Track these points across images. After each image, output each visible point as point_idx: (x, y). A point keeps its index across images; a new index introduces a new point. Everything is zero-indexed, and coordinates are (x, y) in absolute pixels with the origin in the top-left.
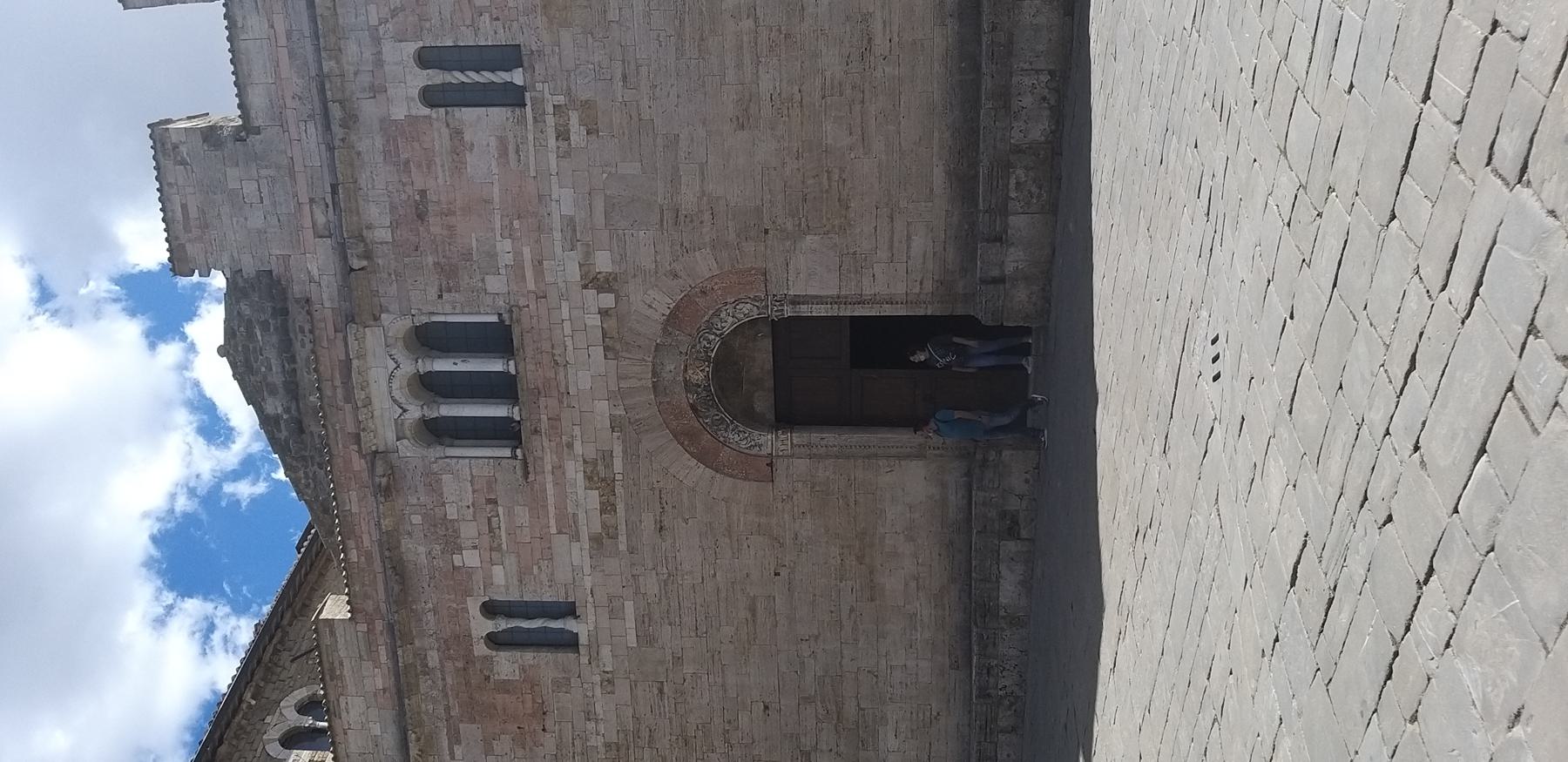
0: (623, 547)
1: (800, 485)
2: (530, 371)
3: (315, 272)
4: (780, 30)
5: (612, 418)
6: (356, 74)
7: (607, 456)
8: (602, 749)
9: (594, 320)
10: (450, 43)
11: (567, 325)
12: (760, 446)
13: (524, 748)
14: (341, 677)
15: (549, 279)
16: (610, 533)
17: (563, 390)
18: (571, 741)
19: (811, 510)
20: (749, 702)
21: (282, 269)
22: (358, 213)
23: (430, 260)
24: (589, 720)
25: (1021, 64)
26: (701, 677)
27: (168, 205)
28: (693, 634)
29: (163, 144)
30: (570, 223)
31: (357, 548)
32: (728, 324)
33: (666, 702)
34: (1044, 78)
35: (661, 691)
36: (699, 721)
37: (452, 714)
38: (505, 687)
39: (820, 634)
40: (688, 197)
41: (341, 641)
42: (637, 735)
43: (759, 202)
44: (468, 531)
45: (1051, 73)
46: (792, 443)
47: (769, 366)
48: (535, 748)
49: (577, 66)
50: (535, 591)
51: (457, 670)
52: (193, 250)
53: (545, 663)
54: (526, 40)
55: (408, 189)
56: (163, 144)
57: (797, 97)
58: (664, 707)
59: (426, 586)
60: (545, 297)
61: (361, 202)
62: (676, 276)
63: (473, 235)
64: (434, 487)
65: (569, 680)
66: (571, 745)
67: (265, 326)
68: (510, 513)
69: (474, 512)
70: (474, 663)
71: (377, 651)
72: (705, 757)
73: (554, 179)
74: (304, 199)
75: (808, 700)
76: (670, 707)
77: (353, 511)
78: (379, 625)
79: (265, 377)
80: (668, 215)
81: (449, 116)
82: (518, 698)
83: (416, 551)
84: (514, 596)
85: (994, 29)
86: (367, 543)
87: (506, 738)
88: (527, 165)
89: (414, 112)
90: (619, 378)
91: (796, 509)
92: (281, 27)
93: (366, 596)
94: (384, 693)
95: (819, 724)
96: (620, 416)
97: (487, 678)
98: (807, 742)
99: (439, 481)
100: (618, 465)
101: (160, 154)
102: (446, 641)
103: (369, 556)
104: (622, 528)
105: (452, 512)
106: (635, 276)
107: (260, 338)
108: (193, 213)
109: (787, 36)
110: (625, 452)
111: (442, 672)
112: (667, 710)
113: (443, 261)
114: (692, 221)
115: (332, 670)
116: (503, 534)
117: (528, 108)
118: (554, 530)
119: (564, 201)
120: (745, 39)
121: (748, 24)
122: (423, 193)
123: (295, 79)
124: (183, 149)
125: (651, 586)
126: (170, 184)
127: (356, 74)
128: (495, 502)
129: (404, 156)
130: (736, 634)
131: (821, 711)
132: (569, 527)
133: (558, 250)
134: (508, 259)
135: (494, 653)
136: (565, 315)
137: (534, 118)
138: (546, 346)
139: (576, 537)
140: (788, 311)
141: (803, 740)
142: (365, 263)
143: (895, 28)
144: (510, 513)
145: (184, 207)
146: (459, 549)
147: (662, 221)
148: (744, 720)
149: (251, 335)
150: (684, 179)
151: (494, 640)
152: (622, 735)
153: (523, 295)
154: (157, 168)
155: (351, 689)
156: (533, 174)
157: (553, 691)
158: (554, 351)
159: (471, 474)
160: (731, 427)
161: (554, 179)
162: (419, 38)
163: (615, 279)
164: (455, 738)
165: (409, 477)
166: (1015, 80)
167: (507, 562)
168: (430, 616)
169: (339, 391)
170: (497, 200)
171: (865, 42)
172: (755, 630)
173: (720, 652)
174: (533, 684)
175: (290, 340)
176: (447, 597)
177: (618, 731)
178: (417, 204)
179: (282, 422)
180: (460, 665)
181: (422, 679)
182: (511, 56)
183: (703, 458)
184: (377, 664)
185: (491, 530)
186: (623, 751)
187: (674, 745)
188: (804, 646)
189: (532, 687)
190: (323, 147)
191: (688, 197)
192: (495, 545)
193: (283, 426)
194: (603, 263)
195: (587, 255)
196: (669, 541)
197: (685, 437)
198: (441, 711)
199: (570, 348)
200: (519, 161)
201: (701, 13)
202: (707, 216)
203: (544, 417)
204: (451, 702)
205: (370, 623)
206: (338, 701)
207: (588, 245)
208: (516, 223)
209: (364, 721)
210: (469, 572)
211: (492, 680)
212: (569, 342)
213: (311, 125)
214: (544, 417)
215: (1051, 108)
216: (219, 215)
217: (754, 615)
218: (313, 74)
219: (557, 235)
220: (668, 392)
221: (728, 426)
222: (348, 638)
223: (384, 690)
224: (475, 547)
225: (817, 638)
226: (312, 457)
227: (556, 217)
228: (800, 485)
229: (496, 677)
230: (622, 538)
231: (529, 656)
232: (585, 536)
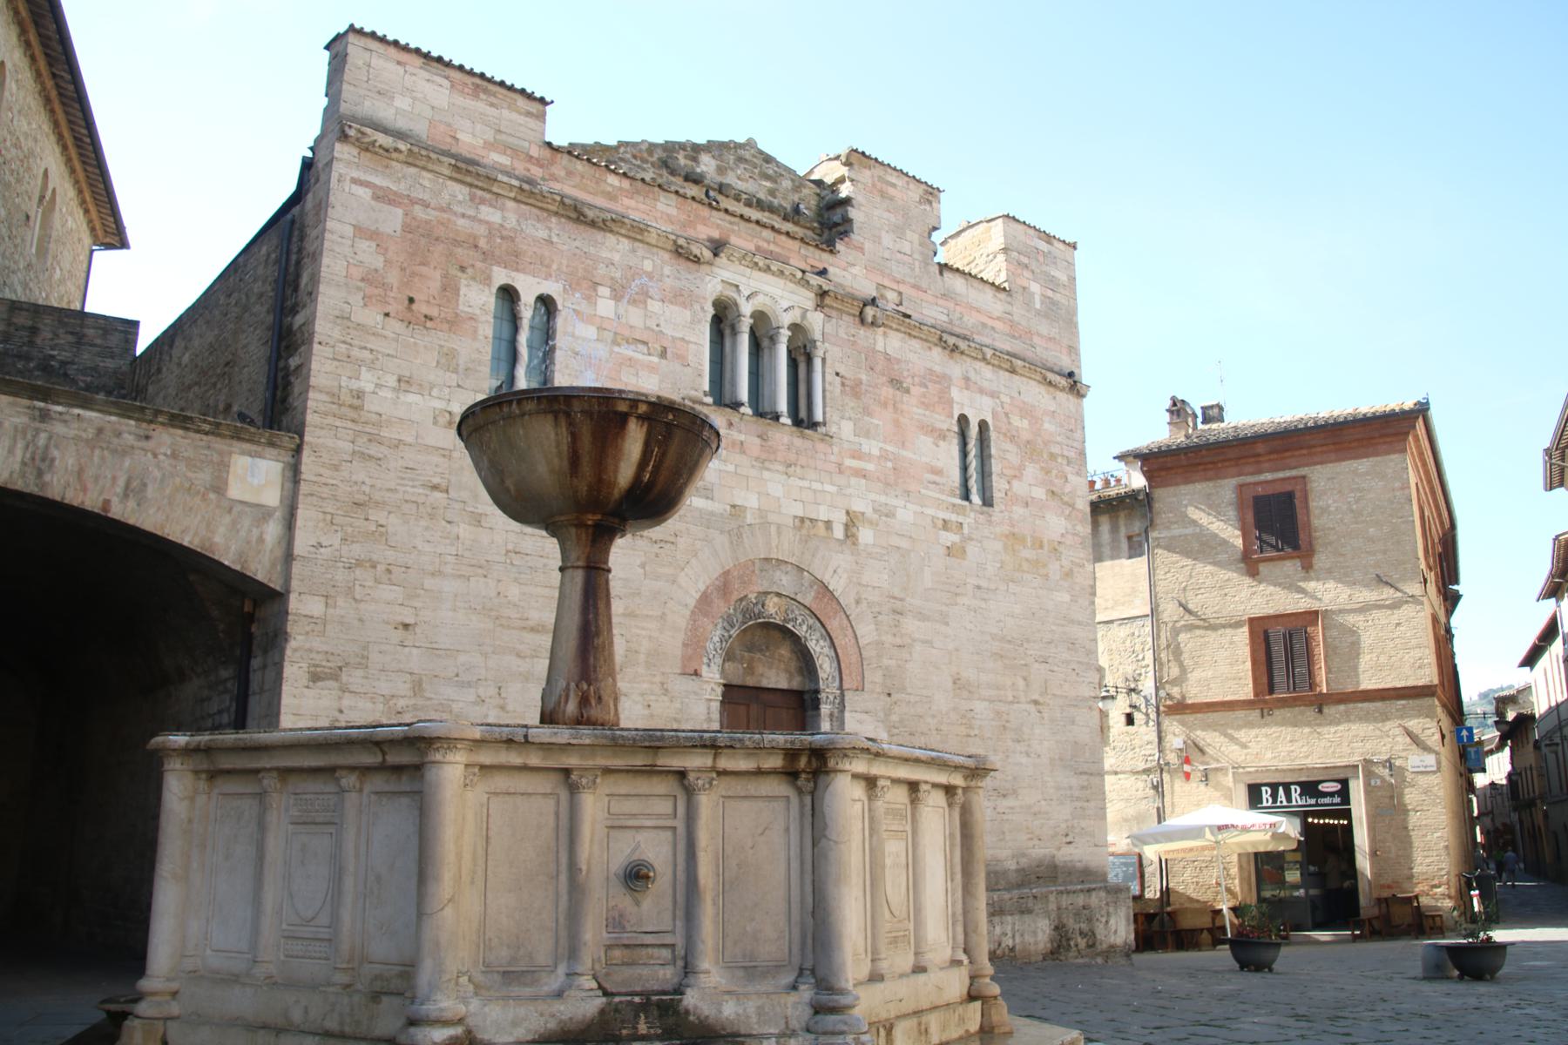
1: (678, 706)
3: (855, 270)
4: (1007, 721)
5: (743, 509)
6: (975, 370)
8: (355, 385)
9: (823, 514)
10: (993, 451)
12: (709, 666)
13: (363, 280)
14: (476, 96)
15: (853, 481)
17: (767, 464)
18: (369, 346)
19: (652, 716)
20: (418, 604)
21: (856, 244)
22: (897, 330)
23: (864, 377)
24: (399, 381)
25: (1017, 923)
26: (452, 545)
27: (895, 173)
28: (510, 547)
29: (931, 194)
31: (621, 189)
32: (817, 646)
33: (421, 491)
34: (1010, 943)
35: (435, 487)
36: (390, 529)
37: (417, 207)
38: (449, 289)
39: (507, 712)
40: (911, 625)
41: (522, 119)
42: (372, 439)
43: (909, 690)
44: (635, 316)
45: (1012, 950)
46: (711, 700)
47: (765, 683)
48: (362, 294)
49: (984, 550)
50: (567, 367)
51: (475, 238)
52: (866, 176)
55: (909, 380)
56: (931, 194)
58: (413, 487)
59: (577, 243)
60: (840, 472)
61: (903, 335)
62: (858, 602)
63: (881, 423)
64: (679, 298)
65: (456, 371)
66: (363, 344)
67: (772, 192)
69: (653, 330)
70: (484, 261)
71: (505, 154)
72: (336, 528)
73: (919, 509)
74: (902, 288)
75: (417, 687)
76: (413, 494)
77: (658, 204)
78: (536, 172)
79: (732, 169)
80: (898, 605)
81: (952, 434)
82: (434, 298)
83: (614, 249)
84: (561, 341)
85: (1035, 897)
86: (626, 201)
87: (379, 262)
88: (927, 488)
89: (955, 405)
90: (779, 526)
91: (653, 698)
92: (998, 325)
93: (570, 173)
94: (451, 136)
95: (381, 699)
96: (745, 517)
97: (463, 269)
98: (354, 678)
99: (684, 305)
101: (926, 188)
102: (512, 239)
103: (612, 197)
105: (654, 306)
106: (857, 563)
107: (764, 183)
108: (891, 191)
109: (1004, 726)
110: (712, 514)
111: (473, 219)
112: (408, 489)
113: (863, 387)
114: (896, 626)
115: (486, 91)
117: (959, 501)
119: (906, 513)
120: (1002, 692)
122: (908, 391)
123: (972, 320)
124: (928, 207)
126: (908, 183)
127: (975, 370)
128: (663, 354)
129: (930, 385)
130: (509, 603)
131: (401, 703)
133: (873, 496)
134: (865, 448)
135: (494, 290)
136: (828, 488)
137: (954, 505)
138: (803, 460)
140: (825, 709)
141: (360, 673)
142: (870, 319)
143: (1010, 817)
144: (652, 369)
145: (894, 186)
146: (617, 296)
147: (895, 598)
148: (387, 592)
149: (767, 177)
151: (508, 294)
152: (374, 418)
153: (840, 452)
154: (919, 181)
155: (460, 100)
156: (923, 491)
157: (441, 346)
158: (799, 467)
159: (692, 342)
160: (726, 634)
161: (919, 509)
162: (995, 427)
163: (854, 544)
164: (382, 196)
165: (689, 277)
166: (1009, 918)
167: (600, 345)
168: (542, 233)
169: (765, 245)
170: (904, 453)
171: (1002, 792)
172: (513, 628)
173: (485, 576)
174: (454, 323)
175: (764, 211)
176: (565, 262)
177: (380, 415)
178: (901, 383)
179: (694, 164)
180: (482, 243)
181: (466, 190)
182: (987, 502)
183: (705, 599)
184: (489, 146)
186: (353, 414)
187: (355, 488)
188: (493, 691)
189: (448, 322)
190: (933, 321)
191: (911, 625)
192: (619, 340)
193: (689, 163)
194: (865, 535)
195: (871, 523)
197: (724, 585)
198: (418, 194)
199: (801, 483)
200: (929, 482)
201: (1015, 659)
202: (898, 641)
203: (742, 437)
204: (433, 212)
205: (538, 162)
206: (447, 78)
207: (877, 525)
208: (889, 464)
209: (414, 94)
210: (591, 299)
211: (460, 274)
212: (806, 484)
213: (945, 318)
215: (995, 952)
216: (889, 212)
217: (532, 630)
218: (975, 336)
219: (883, 499)
220: (764, 573)
221: (728, 631)
222: (522, 129)
223: (457, 140)
226: (661, 176)
227: (895, 502)
228: (678, 706)
229: (463, 282)
231: (487, 328)
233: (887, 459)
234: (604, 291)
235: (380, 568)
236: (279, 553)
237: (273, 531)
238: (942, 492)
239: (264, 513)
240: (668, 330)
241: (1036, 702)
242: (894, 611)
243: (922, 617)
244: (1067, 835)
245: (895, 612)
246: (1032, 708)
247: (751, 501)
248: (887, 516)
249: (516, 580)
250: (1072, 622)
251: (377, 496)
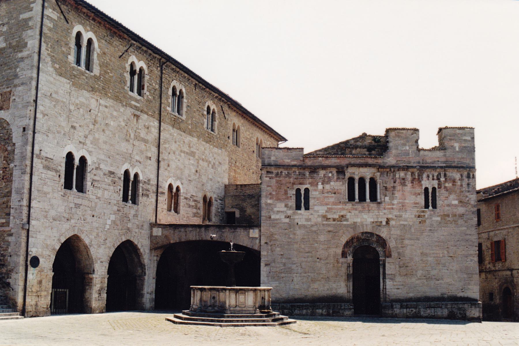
0: (324, 222)
2: (365, 204)
5: (356, 222)
7: (347, 220)
11: (378, 214)
16: (328, 219)
30: (401, 216)
40: (406, 242)
44: (327, 187)
53: (292, 203)
54: (437, 210)
57: (427, 265)
62: (390, 238)
68: (332, 197)
80: (403, 238)
90: (366, 225)
100: (345, 223)
104: (329, 223)
105: (332, 183)
109: (439, 264)
110: (348, 225)
116: (327, 195)
118: (328, 206)
120: (438, 255)
121: (441, 255)
125: (314, 229)
128: (335, 193)
132: (329, 210)
139: (326, 212)
144: (332, 197)
146: (322, 184)
148: (278, 249)
150: (410, 241)
174: (287, 198)
182: (434, 206)
183: (347, 244)
185: (328, 192)
188: (299, 264)
194: (392, 223)
196: (326, 233)
203: (356, 207)
212: (374, 214)
214: (356, 207)
217: (307, 253)
224: (323, 188)
225: (301, 267)
227: (401, 213)
230: (326, 223)
231: (294, 198)
232: (327, 214)
233: (399, 204)
234: (320, 183)
235: (276, 245)
236: (259, 245)
237: (258, 241)
238: (418, 208)
239: (256, 238)
240: (336, 188)
241: (451, 257)
242: (401, 239)
243: (411, 239)
244: (462, 290)
245: (401, 239)
246: (450, 258)
247: (359, 220)
248: (399, 217)
249: (303, 244)
250: (467, 235)
251: (275, 233)
